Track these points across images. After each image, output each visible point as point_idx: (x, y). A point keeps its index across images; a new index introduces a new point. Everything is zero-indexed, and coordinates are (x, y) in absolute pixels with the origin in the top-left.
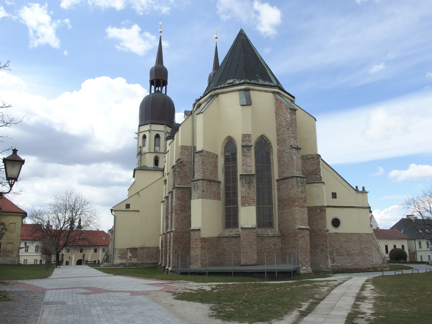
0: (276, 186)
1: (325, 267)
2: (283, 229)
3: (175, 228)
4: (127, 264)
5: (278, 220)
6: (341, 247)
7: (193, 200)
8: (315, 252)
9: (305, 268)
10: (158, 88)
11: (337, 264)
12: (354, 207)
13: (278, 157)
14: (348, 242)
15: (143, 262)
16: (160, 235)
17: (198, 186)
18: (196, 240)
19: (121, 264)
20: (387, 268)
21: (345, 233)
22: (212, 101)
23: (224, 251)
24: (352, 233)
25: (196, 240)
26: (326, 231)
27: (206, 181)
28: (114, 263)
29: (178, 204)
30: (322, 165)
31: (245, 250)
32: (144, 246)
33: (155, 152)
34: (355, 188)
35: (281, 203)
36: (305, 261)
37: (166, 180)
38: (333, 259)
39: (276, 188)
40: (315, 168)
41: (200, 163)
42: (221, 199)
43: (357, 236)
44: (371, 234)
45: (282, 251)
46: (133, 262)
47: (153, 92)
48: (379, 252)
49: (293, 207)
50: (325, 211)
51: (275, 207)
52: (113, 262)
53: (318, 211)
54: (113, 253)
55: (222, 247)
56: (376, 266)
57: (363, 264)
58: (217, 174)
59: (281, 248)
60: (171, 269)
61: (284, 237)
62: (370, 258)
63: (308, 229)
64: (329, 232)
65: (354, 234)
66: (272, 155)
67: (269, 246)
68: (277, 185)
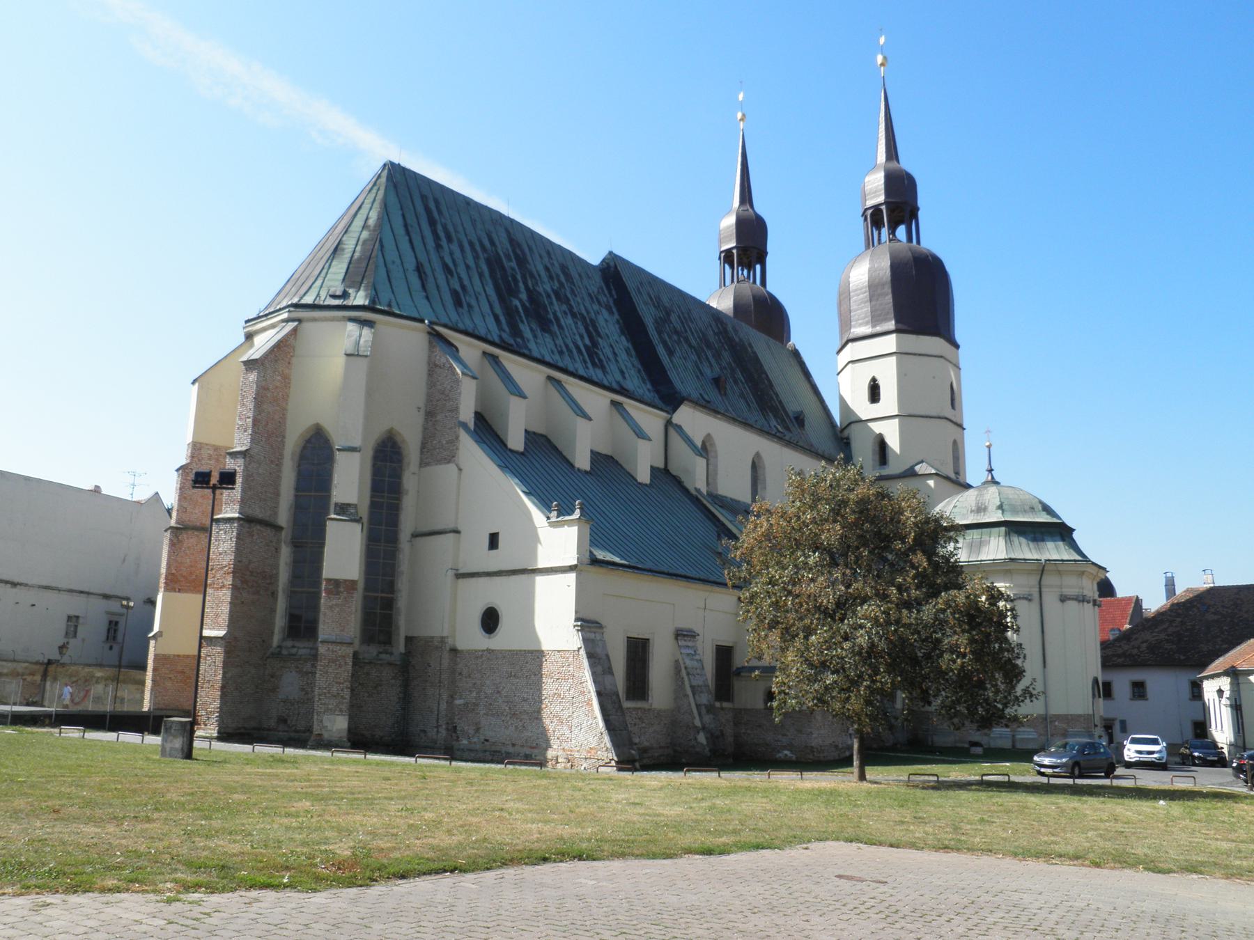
6: (498, 692)
38: (476, 724)
62: (565, 729)
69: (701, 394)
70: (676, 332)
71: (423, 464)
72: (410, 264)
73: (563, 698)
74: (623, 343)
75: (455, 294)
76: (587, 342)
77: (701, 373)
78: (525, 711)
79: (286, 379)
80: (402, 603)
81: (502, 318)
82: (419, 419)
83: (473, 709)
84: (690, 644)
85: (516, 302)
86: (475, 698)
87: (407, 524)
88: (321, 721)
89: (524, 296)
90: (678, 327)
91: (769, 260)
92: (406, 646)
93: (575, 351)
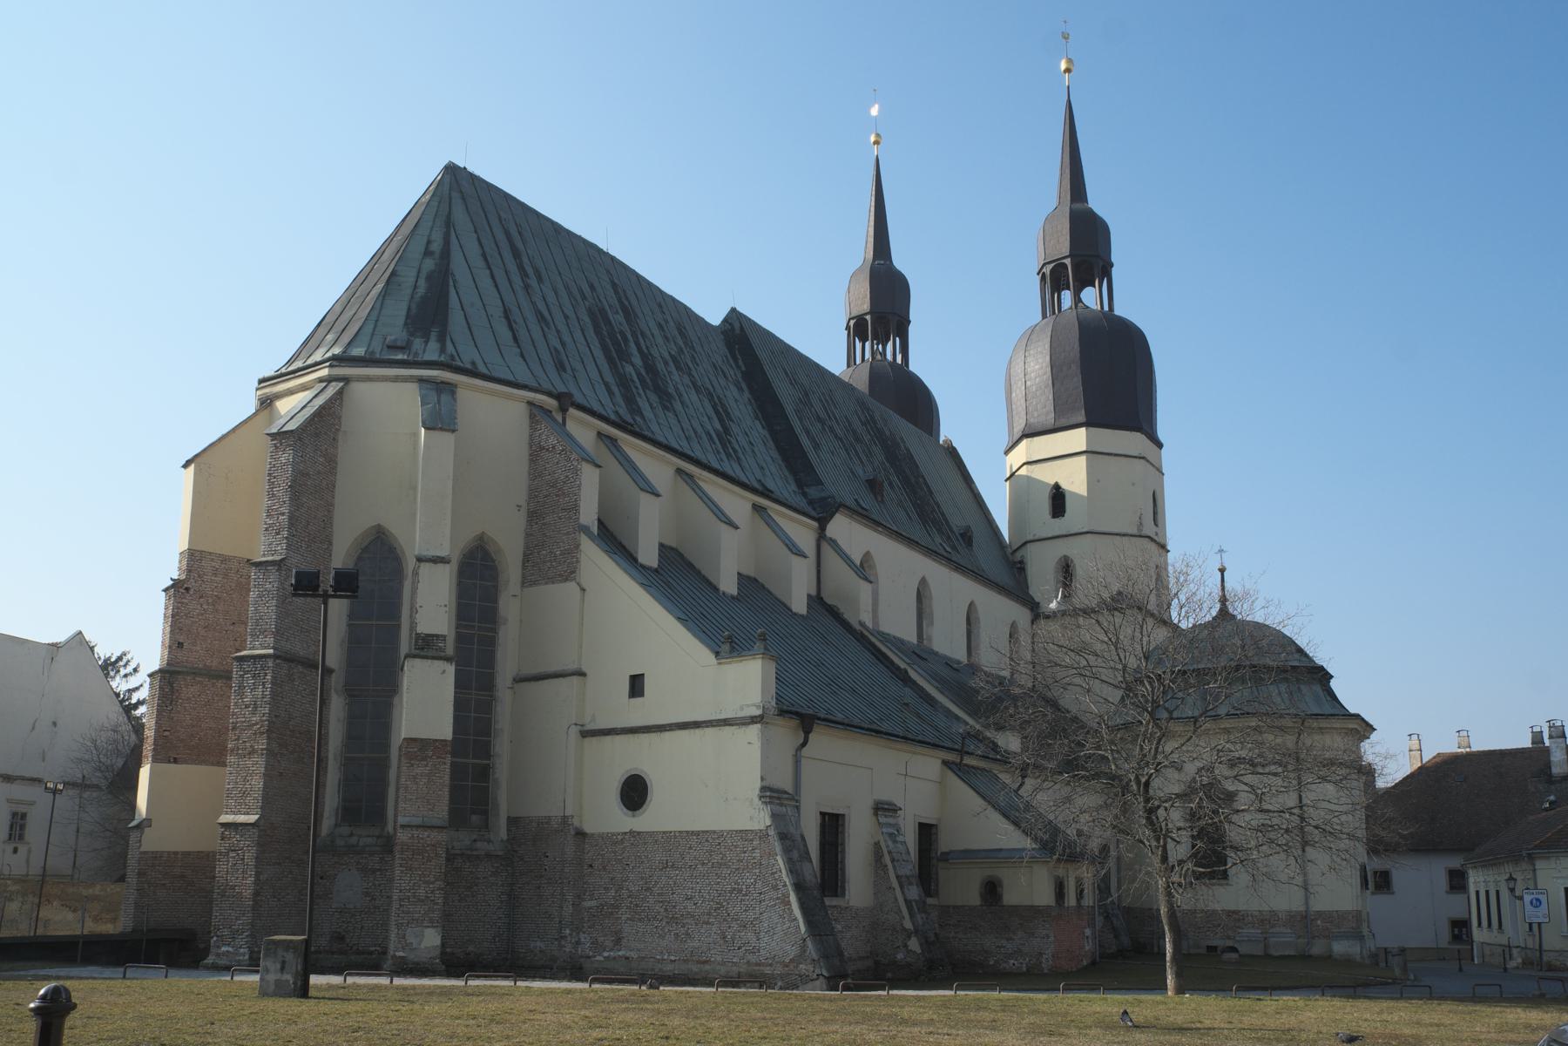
11: (627, 955)
12: (696, 725)
14: (673, 866)
21: (664, 832)
24: (687, 832)
48: (788, 909)
56: (768, 970)
62: (751, 936)
65: (697, 833)
69: (856, 500)
70: (819, 419)
71: (526, 582)
72: (496, 311)
73: (746, 895)
74: (758, 431)
75: (555, 353)
76: (718, 426)
77: (853, 473)
78: (689, 913)
79: (332, 462)
80: (502, 770)
81: (615, 389)
82: (519, 521)
83: (612, 913)
84: (891, 820)
85: (629, 369)
86: (614, 897)
87: (507, 665)
88: (404, 937)
89: (637, 360)
90: (822, 415)
91: (913, 331)
92: (508, 830)
93: (704, 435)
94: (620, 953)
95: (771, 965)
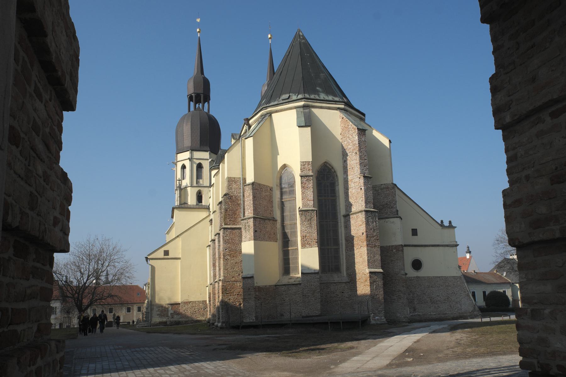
0: (343, 223)
1: (402, 316)
2: (352, 273)
3: (224, 276)
4: (168, 323)
5: (346, 263)
6: (424, 294)
7: (243, 242)
8: (391, 300)
9: (379, 318)
10: (199, 104)
11: (418, 314)
12: (438, 246)
13: (344, 188)
15: (187, 320)
16: (207, 287)
17: (249, 226)
18: (249, 289)
19: (161, 323)
20: (478, 316)
21: (428, 277)
22: (263, 122)
23: (283, 302)
25: (249, 289)
26: (403, 275)
27: (258, 220)
28: (152, 321)
29: (226, 248)
30: (398, 195)
31: (306, 299)
32: (188, 300)
33: (197, 186)
34: (440, 222)
35: (349, 242)
36: (379, 310)
37: (211, 220)
39: (343, 226)
40: (389, 200)
41: (251, 197)
42: (278, 241)
43: (443, 279)
44: (460, 277)
45: (351, 300)
46: (176, 320)
47: (192, 109)
49: (363, 247)
50: (402, 251)
51: (342, 247)
52: (151, 321)
53: (394, 251)
54: (151, 310)
55: (280, 297)
56: (465, 314)
57: (450, 312)
58: (272, 211)
59: (350, 295)
60: (221, 325)
61: (353, 283)
63: (381, 272)
64: (407, 276)
66: (338, 185)
67: (336, 294)
68: (344, 222)
73: (456, 294)
78: (438, 300)
86: (412, 297)
94: (416, 314)
95: (466, 313)
